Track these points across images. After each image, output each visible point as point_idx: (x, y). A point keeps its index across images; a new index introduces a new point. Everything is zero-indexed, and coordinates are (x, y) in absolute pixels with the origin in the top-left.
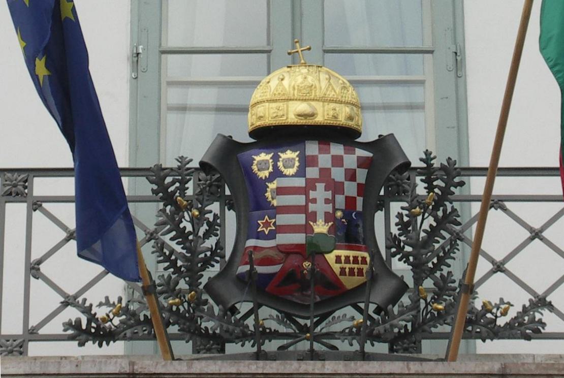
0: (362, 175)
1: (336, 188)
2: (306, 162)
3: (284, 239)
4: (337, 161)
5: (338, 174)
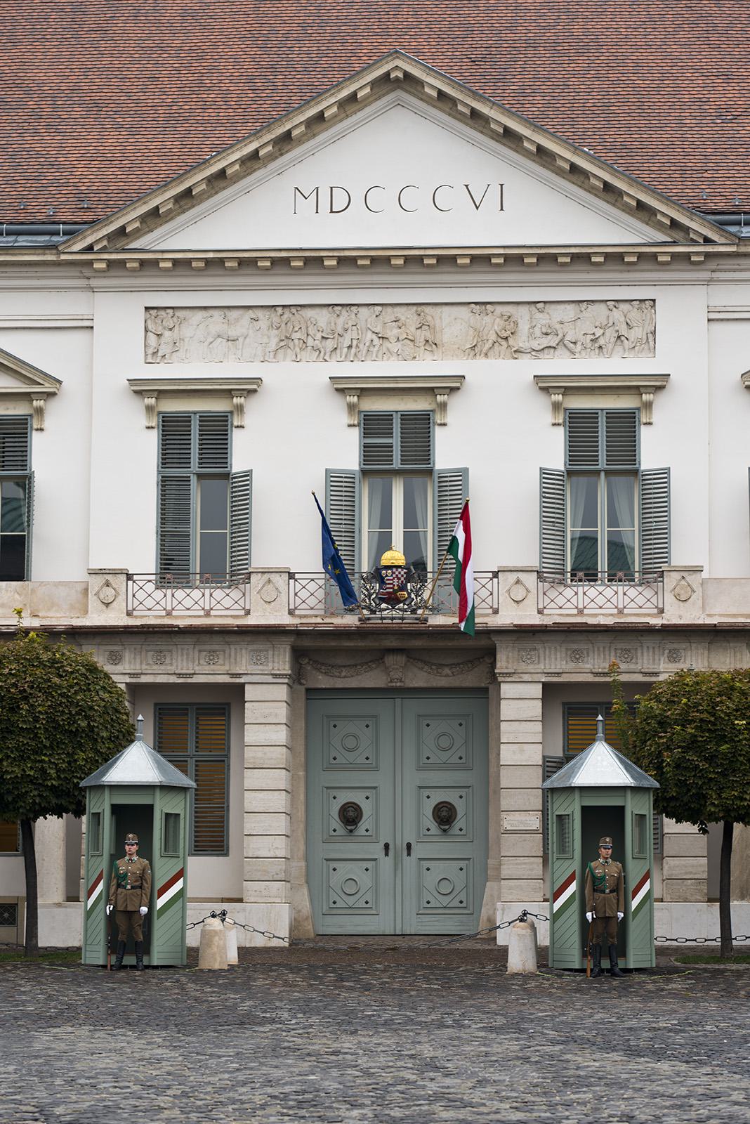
0: (405, 576)
1: (399, 579)
2: (393, 573)
3: (388, 590)
4: (400, 573)
5: (400, 576)
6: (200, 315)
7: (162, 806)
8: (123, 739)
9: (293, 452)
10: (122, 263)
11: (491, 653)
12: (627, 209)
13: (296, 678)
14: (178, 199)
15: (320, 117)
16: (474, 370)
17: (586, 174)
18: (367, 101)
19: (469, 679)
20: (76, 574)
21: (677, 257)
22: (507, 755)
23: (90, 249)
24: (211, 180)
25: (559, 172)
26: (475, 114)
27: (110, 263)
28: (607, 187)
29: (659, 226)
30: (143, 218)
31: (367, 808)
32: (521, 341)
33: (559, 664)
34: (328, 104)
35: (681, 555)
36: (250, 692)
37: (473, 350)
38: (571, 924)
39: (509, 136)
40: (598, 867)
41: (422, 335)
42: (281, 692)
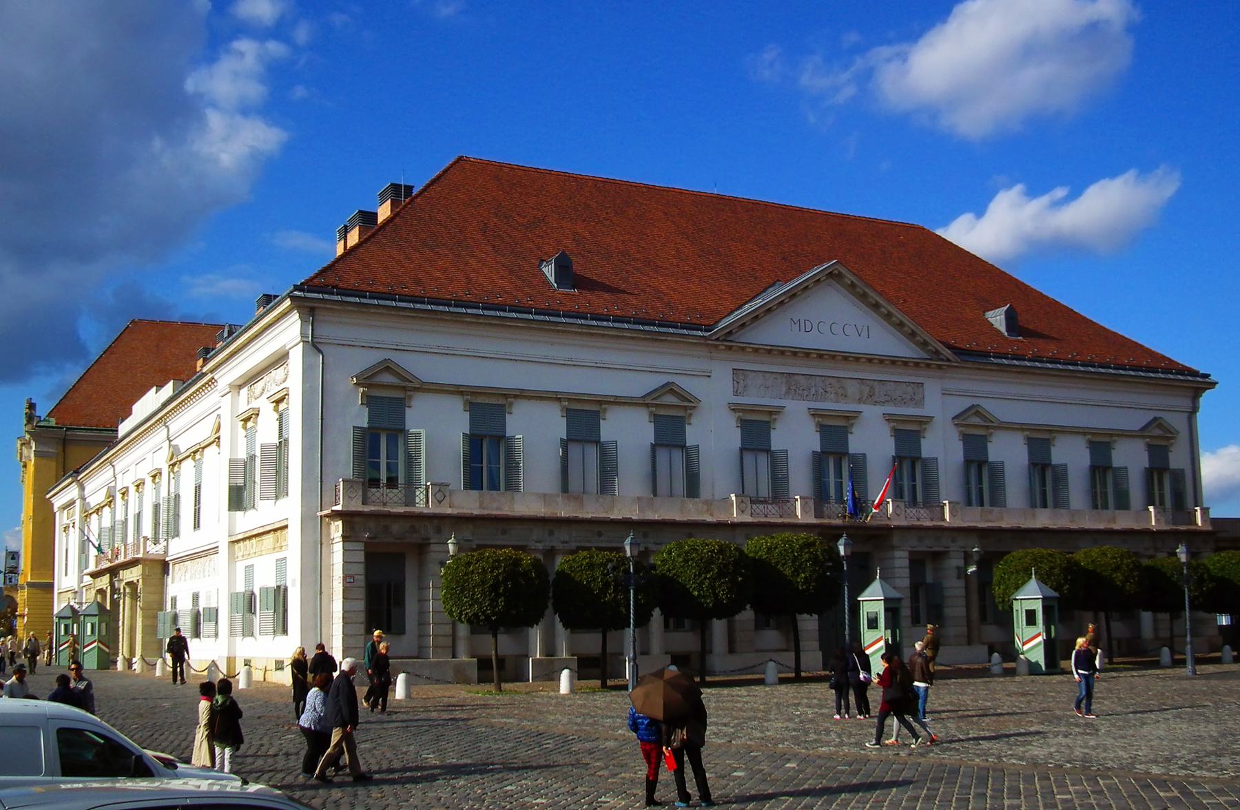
6: (754, 374)
21: (933, 363)
23: (717, 339)
29: (929, 352)
33: (913, 543)
37: (860, 401)
41: (840, 391)
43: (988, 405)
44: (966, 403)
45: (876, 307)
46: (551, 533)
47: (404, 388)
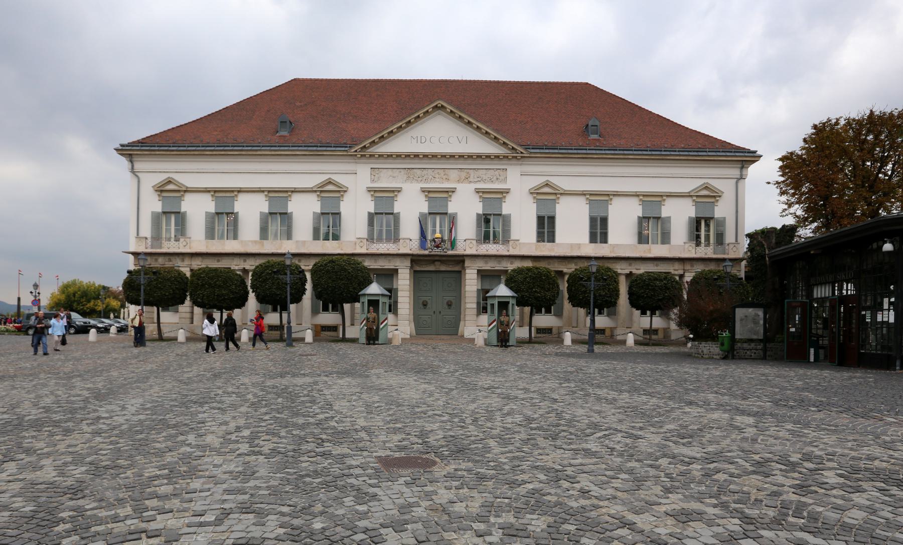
7: (382, 300)
8: (370, 282)
9: (411, 207)
10: (364, 156)
11: (463, 262)
12: (500, 144)
13: (411, 267)
14: (380, 138)
15: (418, 116)
16: (459, 187)
17: (489, 134)
18: (431, 112)
19: (456, 269)
20: (353, 239)
21: (514, 157)
22: (468, 288)
24: (389, 133)
25: (482, 133)
26: (460, 117)
27: (362, 156)
28: (495, 138)
30: (371, 143)
31: (429, 302)
32: (471, 179)
34: (420, 113)
35: (513, 237)
36: (400, 271)
38: (494, 332)
39: (469, 123)
40: (502, 318)
41: (444, 177)
42: (408, 271)
43: (555, 181)
44: (542, 180)
45: (469, 123)
46: (245, 261)
47: (178, 191)
